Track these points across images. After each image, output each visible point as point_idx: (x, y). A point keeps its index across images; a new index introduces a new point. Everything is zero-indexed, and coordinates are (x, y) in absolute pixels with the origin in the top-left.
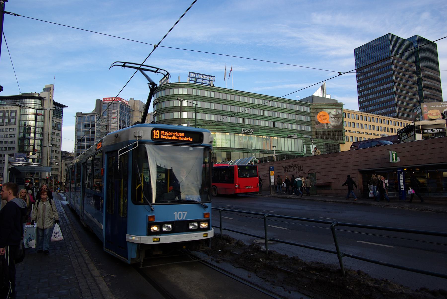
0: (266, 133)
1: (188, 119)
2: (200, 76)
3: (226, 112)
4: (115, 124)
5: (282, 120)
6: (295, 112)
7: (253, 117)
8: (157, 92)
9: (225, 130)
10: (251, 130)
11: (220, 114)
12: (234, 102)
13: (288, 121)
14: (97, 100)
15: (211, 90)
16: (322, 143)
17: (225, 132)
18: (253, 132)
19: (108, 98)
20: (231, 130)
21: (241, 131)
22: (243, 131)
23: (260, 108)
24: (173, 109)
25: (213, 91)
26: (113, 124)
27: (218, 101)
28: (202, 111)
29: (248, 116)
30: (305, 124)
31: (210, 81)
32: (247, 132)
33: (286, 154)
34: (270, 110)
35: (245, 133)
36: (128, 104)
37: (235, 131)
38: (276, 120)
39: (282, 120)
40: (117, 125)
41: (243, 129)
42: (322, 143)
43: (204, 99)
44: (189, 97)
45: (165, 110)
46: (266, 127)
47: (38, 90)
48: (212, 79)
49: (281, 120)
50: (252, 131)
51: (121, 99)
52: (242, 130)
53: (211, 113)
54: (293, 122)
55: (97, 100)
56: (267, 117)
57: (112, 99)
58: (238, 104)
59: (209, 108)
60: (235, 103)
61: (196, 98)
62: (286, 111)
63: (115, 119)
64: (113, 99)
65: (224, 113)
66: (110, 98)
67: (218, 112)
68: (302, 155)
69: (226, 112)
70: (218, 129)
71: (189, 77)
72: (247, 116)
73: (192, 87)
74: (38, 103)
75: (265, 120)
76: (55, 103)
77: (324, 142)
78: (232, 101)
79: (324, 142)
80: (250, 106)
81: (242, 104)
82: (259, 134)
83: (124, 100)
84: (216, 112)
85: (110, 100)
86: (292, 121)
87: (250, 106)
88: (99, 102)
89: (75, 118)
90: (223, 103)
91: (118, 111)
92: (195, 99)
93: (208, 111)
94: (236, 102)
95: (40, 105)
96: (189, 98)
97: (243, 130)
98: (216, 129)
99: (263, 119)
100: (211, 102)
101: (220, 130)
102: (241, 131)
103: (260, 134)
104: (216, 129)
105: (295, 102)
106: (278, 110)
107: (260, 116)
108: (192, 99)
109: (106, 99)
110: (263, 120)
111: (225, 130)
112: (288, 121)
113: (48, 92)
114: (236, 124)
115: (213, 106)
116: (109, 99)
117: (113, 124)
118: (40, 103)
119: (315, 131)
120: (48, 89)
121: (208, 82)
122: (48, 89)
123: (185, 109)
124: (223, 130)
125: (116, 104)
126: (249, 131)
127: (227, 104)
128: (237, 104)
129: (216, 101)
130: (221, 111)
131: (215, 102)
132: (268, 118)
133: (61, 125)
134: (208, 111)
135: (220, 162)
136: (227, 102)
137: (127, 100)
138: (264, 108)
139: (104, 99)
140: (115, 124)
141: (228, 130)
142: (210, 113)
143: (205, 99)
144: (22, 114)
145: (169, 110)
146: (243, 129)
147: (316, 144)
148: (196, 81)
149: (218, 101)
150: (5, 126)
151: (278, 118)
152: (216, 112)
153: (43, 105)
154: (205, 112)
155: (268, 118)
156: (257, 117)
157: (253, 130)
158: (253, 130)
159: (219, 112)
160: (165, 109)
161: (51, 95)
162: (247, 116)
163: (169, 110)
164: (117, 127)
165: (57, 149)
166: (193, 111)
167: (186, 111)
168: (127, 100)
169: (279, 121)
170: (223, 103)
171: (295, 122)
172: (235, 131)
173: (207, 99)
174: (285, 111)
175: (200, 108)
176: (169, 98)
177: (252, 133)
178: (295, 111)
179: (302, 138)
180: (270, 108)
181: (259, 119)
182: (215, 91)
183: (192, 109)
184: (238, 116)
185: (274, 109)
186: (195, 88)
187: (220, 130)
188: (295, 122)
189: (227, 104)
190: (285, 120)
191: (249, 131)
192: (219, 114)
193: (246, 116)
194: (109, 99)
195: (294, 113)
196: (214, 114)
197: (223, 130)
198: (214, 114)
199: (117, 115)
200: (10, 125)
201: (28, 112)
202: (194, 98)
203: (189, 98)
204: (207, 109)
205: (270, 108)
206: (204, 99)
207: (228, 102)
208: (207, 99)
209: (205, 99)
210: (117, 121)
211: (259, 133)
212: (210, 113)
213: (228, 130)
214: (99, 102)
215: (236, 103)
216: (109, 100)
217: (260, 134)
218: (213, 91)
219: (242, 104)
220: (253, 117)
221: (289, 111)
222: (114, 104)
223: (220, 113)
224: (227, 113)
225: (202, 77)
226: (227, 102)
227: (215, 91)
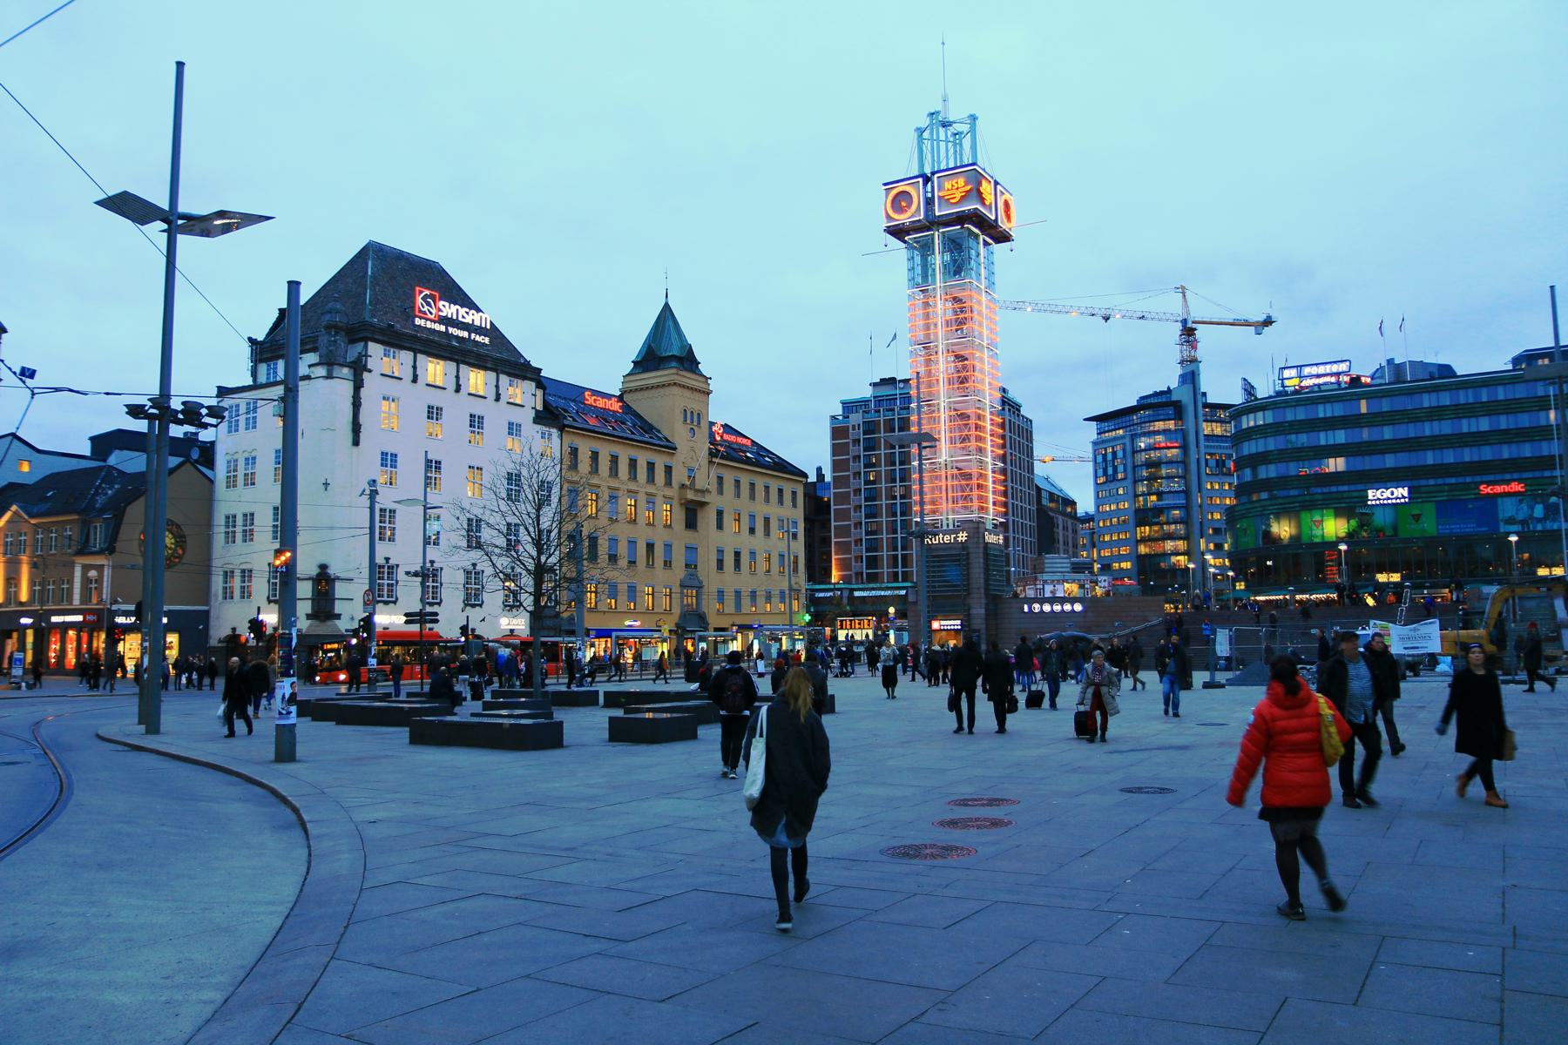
0: (1446, 494)
1: (1276, 480)
9: (1320, 502)
20: (1337, 501)
34: (1536, 408)
37: (1347, 501)
65: (1372, 448)
67: (1355, 449)
75: (1515, 440)
94: (1409, 412)
101: (1308, 503)
103: (1424, 499)
104: (1297, 505)
111: (1320, 502)
144: (1137, 451)
172: (1347, 501)
187: (1308, 503)
207: (1386, 418)
217: (1424, 499)
226: (1381, 419)
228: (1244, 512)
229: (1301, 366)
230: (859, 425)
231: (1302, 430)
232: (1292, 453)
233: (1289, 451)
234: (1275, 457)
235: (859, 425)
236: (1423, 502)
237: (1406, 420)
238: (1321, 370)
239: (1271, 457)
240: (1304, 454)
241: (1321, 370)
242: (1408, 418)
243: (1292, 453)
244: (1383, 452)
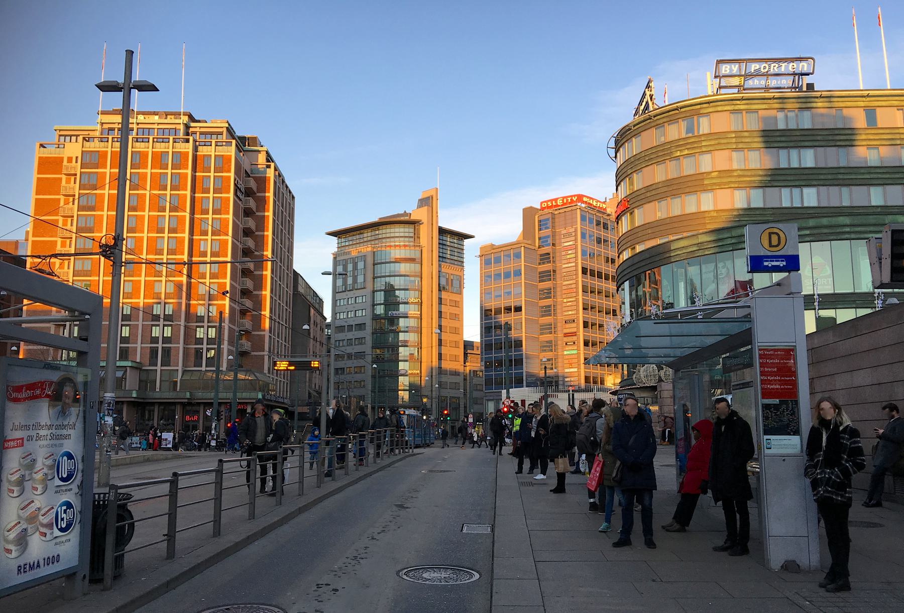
2: (758, 68)
3: (862, 171)
4: (570, 265)
8: (620, 147)
9: (848, 229)
11: (841, 182)
12: (897, 131)
14: (525, 210)
17: (847, 236)
19: (551, 201)
24: (666, 189)
26: (566, 266)
27: (830, 138)
31: (797, 77)
36: (605, 209)
40: (576, 266)
43: (773, 139)
44: (716, 142)
45: (642, 197)
47: (407, 205)
48: (804, 67)
51: (585, 199)
55: (525, 210)
57: (561, 201)
61: (744, 140)
63: (570, 252)
64: (563, 200)
66: (556, 200)
69: (862, 171)
71: (716, 77)
74: (407, 235)
76: (442, 231)
78: (888, 131)
83: (593, 199)
84: (822, 177)
85: (557, 206)
88: (529, 213)
89: (479, 258)
91: (576, 231)
93: (792, 178)
95: (412, 239)
96: (719, 144)
98: (808, 232)
100: (803, 144)
101: (825, 231)
104: (808, 232)
109: (547, 205)
111: (848, 229)
113: (426, 207)
115: (808, 158)
116: (554, 202)
117: (566, 266)
118: (412, 235)
120: (427, 202)
121: (786, 82)
122: (427, 202)
123: (706, 182)
125: (563, 214)
130: (842, 171)
133: (460, 282)
134: (792, 178)
135: (396, 320)
137: (606, 198)
139: (541, 203)
140: (570, 265)
142: (797, 183)
143: (778, 139)
145: (653, 193)
148: (743, 86)
149: (830, 138)
150: (347, 293)
152: (822, 177)
153: (416, 236)
160: (643, 191)
161: (433, 215)
163: (653, 193)
164: (576, 270)
165: (454, 337)
166: (733, 186)
168: (606, 198)
173: (783, 139)
176: (652, 157)
187: (825, 231)
194: (554, 202)
196: (815, 183)
198: (815, 183)
199: (576, 240)
200: (356, 289)
201: (383, 257)
202: (734, 140)
203: (719, 144)
204: (788, 172)
206: (773, 139)
207: (871, 137)
208: (783, 139)
209: (778, 139)
210: (576, 257)
212: (797, 183)
214: (529, 213)
216: (554, 204)
222: (567, 213)
223: (840, 177)
224: (868, 176)
225: (762, 70)
228: (695, 249)
230: (77, 157)
232: (739, 176)
233: (735, 174)
234: (714, 181)
235: (77, 157)
238: (774, 68)
239: (706, 182)
241: (774, 68)
244: (869, 183)
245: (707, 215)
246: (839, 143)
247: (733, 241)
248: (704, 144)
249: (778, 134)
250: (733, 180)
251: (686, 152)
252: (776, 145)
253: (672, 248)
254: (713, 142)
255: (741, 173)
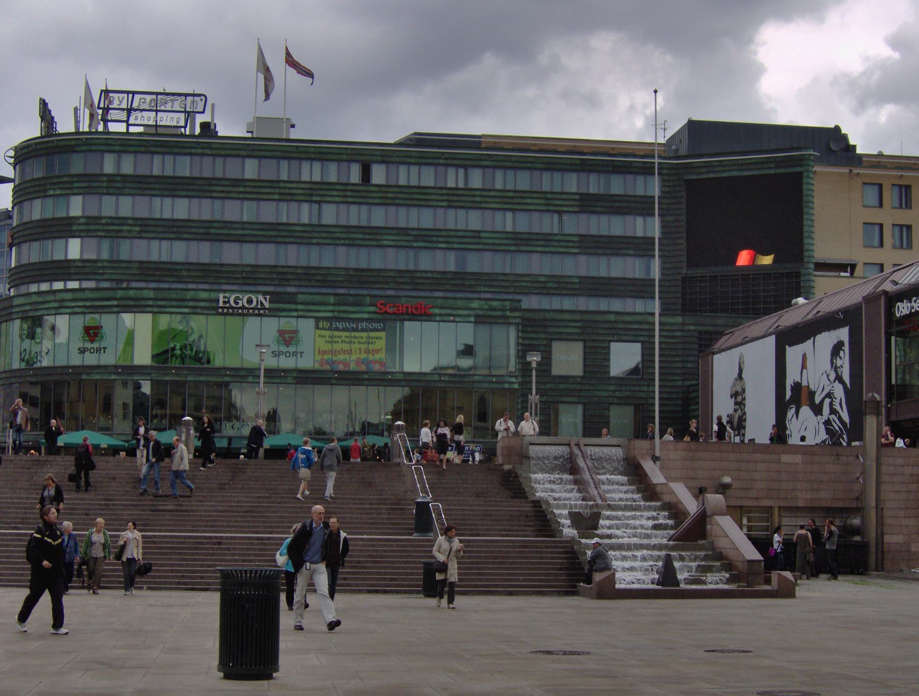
0: (330, 308)
1: (80, 264)
5: (506, 242)
6: (578, 203)
7: (361, 236)
9: (151, 303)
10: (261, 298)
13: (533, 243)
15: (176, 150)
16: (678, 334)
18: (267, 305)
20: (174, 303)
21: (214, 305)
22: (221, 304)
23: (397, 201)
25: (187, 151)
28: (138, 229)
29: (338, 235)
30: (631, 252)
32: (240, 305)
33: (423, 384)
34: (445, 204)
35: (231, 311)
37: (191, 304)
38: (476, 240)
39: (506, 242)
41: (221, 296)
42: (678, 334)
43: (146, 186)
46: (418, 275)
49: (497, 241)
50: (261, 303)
52: (218, 301)
53: (173, 236)
54: (563, 244)
56: (428, 233)
58: (293, 191)
59: (164, 216)
60: (277, 191)
62: (530, 201)
65: (226, 232)
67: (202, 231)
68: (507, 386)
70: (123, 303)
72: (330, 235)
73: (100, 148)
75: (415, 244)
77: (692, 328)
78: (268, 184)
79: (692, 328)
80: (349, 194)
81: (309, 192)
82: (296, 310)
84: (193, 230)
86: (555, 244)
87: (349, 194)
90: (224, 195)
92: (111, 191)
94: (282, 185)
97: (221, 300)
98: (115, 303)
99: (407, 244)
101: (131, 303)
102: (214, 305)
103: (301, 313)
104: (115, 303)
105: (578, 162)
106: (488, 203)
107: (395, 232)
108: (100, 190)
110: (407, 247)
111: (151, 303)
112: (539, 243)
114: (280, 270)
119: (679, 277)
123: (75, 228)
124: (143, 303)
126: (250, 301)
127: (242, 196)
128: (287, 191)
129: (195, 187)
130: (215, 225)
131: (192, 193)
132: (435, 239)
134: (161, 229)
136: (241, 189)
138: (416, 196)
141: (160, 303)
142: (167, 236)
146: (225, 297)
147: (641, 339)
151: (483, 235)
152: (193, 230)
154: (149, 235)
155: (435, 239)
156: (378, 237)
157: (268, 297)
158: (268, 297)
159: (209, 228)
162: (330, 235)
166: (100, 234)
167: (77, 234)
169: (487, 247)
170: (224, 195)
171: (571, 244)
172: (191, 304)
173: (157, 186)
174: (520, 201)
175: (130, 222)
177: (262, 312)
178: (577, 197)
179: (512, 321)
180: (446, 198)
181: (386, 243)
182: (193, 151)
183: (97, 227)
184: (288, 240)
185: (464, 198)
186: (111, 148)
187: (131, 303)
188: (571, 244)
189: (242, 196)
190: (519, 242)
191: (250, 301)
192: (208, 237)
193: (325, 235)
195: (570, 209)
196: (186, 236)
197: (143, 303)
202: (105, 184)
205: (446, 198)
209: (152, 186)
211: (300, 307)
212: (167, 236)
213: (160, 303)
215: (282, 191)
217: (301, 313)
218: (187, 151)
219: (309, 192)
220: (361, 236)
221: (544, 202)
224: (240, 232)
226: (241, 189)
227: (193, 151)
228: (28, 308)
229: (134, 93)
231: (127, 191)
232: (107, 224)
233: (104, 221)
234: (81, 228)
236: (298, 317)
237: (277, 197)
239: (75, 228)
240: (126, 228)
242: (280, 194)
243: (107, 224)
245: (72, 264)
246: (214, 195)
247: (56, 305)
248: (75, 185)
249: (152, 180)
250: (101, 227)
251: (58, 192)
252: (149, 192)
253: (14, 304)
254: (84, 185)
255: (109, 221)
